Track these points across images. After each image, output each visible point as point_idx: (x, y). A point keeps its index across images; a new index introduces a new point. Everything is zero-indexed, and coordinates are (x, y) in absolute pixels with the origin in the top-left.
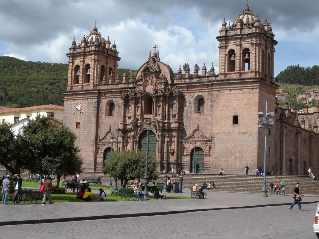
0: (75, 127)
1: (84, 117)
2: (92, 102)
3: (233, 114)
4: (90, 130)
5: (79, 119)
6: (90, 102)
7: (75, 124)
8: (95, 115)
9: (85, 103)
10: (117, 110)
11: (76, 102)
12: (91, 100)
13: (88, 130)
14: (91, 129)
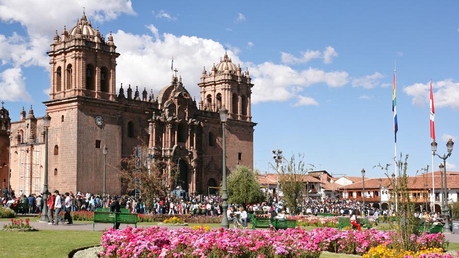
0: (95, 146)
1: (106, 135)
2: (115, 117)
3: (239, 152)
4: (115, 152)
5: (99, 136)
6: (112, 116)
7: (95, 142)
8: (120, 135)
9: (107, 117)
10: (141, 132)
11: (94, 113)
12: (114, 115)
13: (112, 152)
14: (116, 150)
